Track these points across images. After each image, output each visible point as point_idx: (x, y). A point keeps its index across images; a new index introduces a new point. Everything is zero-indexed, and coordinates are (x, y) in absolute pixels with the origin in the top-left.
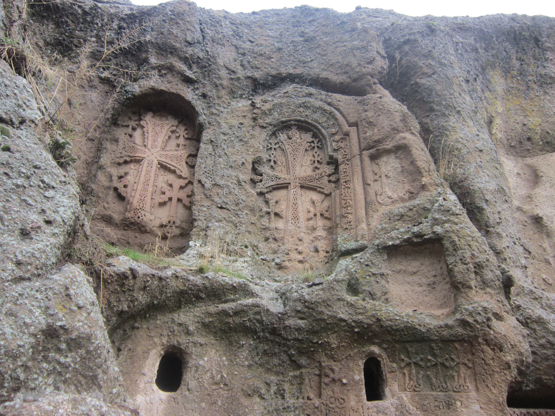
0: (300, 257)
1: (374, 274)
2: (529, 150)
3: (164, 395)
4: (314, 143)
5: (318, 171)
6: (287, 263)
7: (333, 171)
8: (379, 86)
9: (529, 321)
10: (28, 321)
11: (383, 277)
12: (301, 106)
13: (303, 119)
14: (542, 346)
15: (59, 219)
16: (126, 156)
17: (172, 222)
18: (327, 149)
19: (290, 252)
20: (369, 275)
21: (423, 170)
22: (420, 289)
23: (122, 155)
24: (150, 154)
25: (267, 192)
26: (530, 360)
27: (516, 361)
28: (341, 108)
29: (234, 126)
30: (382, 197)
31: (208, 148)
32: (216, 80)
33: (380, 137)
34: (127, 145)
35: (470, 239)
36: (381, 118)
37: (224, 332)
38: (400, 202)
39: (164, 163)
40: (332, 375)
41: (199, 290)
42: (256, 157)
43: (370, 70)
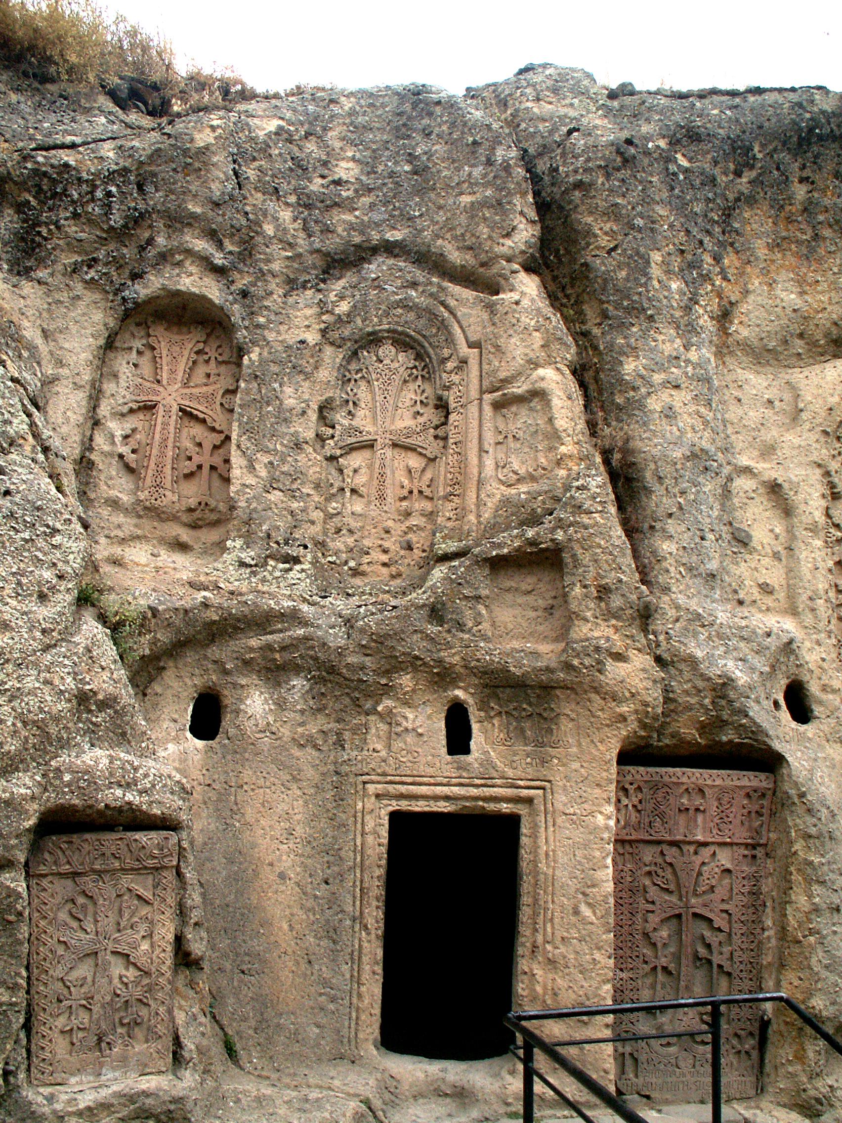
0: (384, 558)
1: (466, 597)
2: (799, 354)
3: (200, 744)
5: (421, 420)
6: (365, 568)
7: (443, 419)
9: (675, 659)
10: (62, 688)
13: (400, 329)
14: (686, 692)
15: (70, 570)
16: (132, 401)
17: (203, 504)
21: (563, 435)
22: (532, 614)
26: (659, 710)
27: (636, 712)
28: (459, 314)
30: (505, 470)
33: (509, 374)
35: (599, 551)
37: (268, 669)
40: (405, 724)
41: (239, 620)
42: (324, 398)
43: (504, 250)
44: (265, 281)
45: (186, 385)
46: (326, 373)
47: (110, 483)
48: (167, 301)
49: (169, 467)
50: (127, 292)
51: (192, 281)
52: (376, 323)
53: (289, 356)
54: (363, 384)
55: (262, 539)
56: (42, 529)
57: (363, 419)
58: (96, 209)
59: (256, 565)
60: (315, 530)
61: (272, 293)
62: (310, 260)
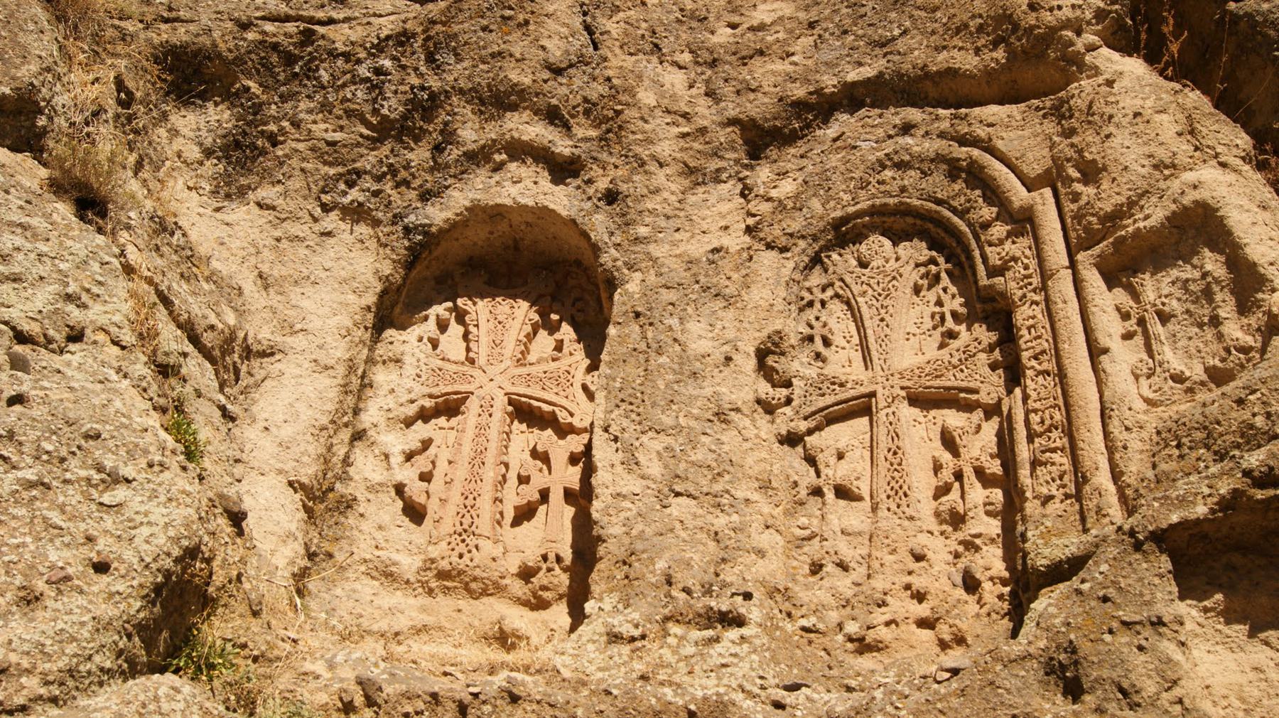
0: (923, 610)
4: (937, 264)
5: (955, 344)
6: (884, 633)
8: (1105, 51)
11: (1163, 630)
12: (884, 167)
13: (891, 201)
15: (129, 555)
17: (552, 557)
18: (974, 274)
19: (888, 599)
20: (1111, 632)
23: (412, 396)
25: (810, 432)
28: (1000, 144)
29: (698, 261)
30: (1155, 379)
32: (638, 150)
34: (424, 367)
36: (1115, 142)
38: (1212, 386)
39: (523, 399)
42: (765, 333)
44: (646, 172)
46: (766, 293)
50: (412, 218)
52: (845, 202)
54: (837, 307)
57: (843, 361)
58: (359, 94)
59: (643, 637)
60: (771, 568)
62: (723, 135)
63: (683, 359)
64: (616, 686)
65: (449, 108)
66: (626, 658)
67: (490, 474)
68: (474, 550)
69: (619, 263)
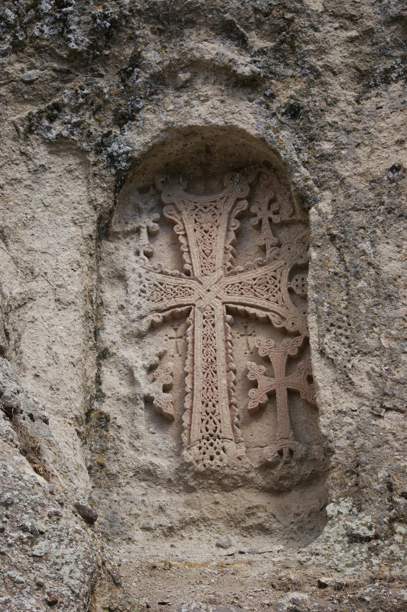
15: (66, 592)
23: (141, 312)
24: (203, 292)
31: (328, 259)
32: (313, 60)
34: (146, 283)
39: (240, 307)
44: (322, 83)
45: (230, 272)
47: (137, 443)
48: (179, 146)
49: (224, 402)
50: (115, 146)
51: (206, 109)
53: (379, 195)
55: (380, 493)
56: (15, 535)
58: (46, 29)
59: (376, 537)
61: (336, 101)
62: (388, 35)
63: (379, 282)
64: (367, 594)
65: (130, 32)
66: (365, 555)
67: (223, 382)
68: (222, 452)
69: (310, 182)
